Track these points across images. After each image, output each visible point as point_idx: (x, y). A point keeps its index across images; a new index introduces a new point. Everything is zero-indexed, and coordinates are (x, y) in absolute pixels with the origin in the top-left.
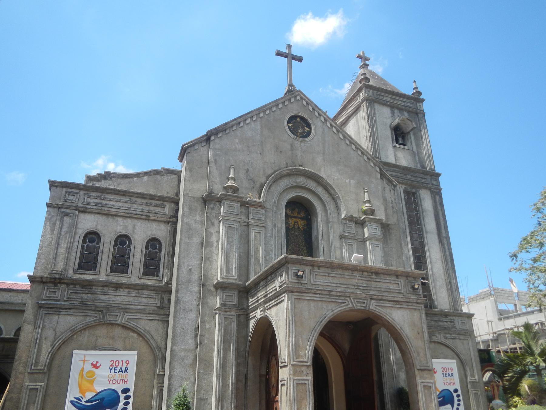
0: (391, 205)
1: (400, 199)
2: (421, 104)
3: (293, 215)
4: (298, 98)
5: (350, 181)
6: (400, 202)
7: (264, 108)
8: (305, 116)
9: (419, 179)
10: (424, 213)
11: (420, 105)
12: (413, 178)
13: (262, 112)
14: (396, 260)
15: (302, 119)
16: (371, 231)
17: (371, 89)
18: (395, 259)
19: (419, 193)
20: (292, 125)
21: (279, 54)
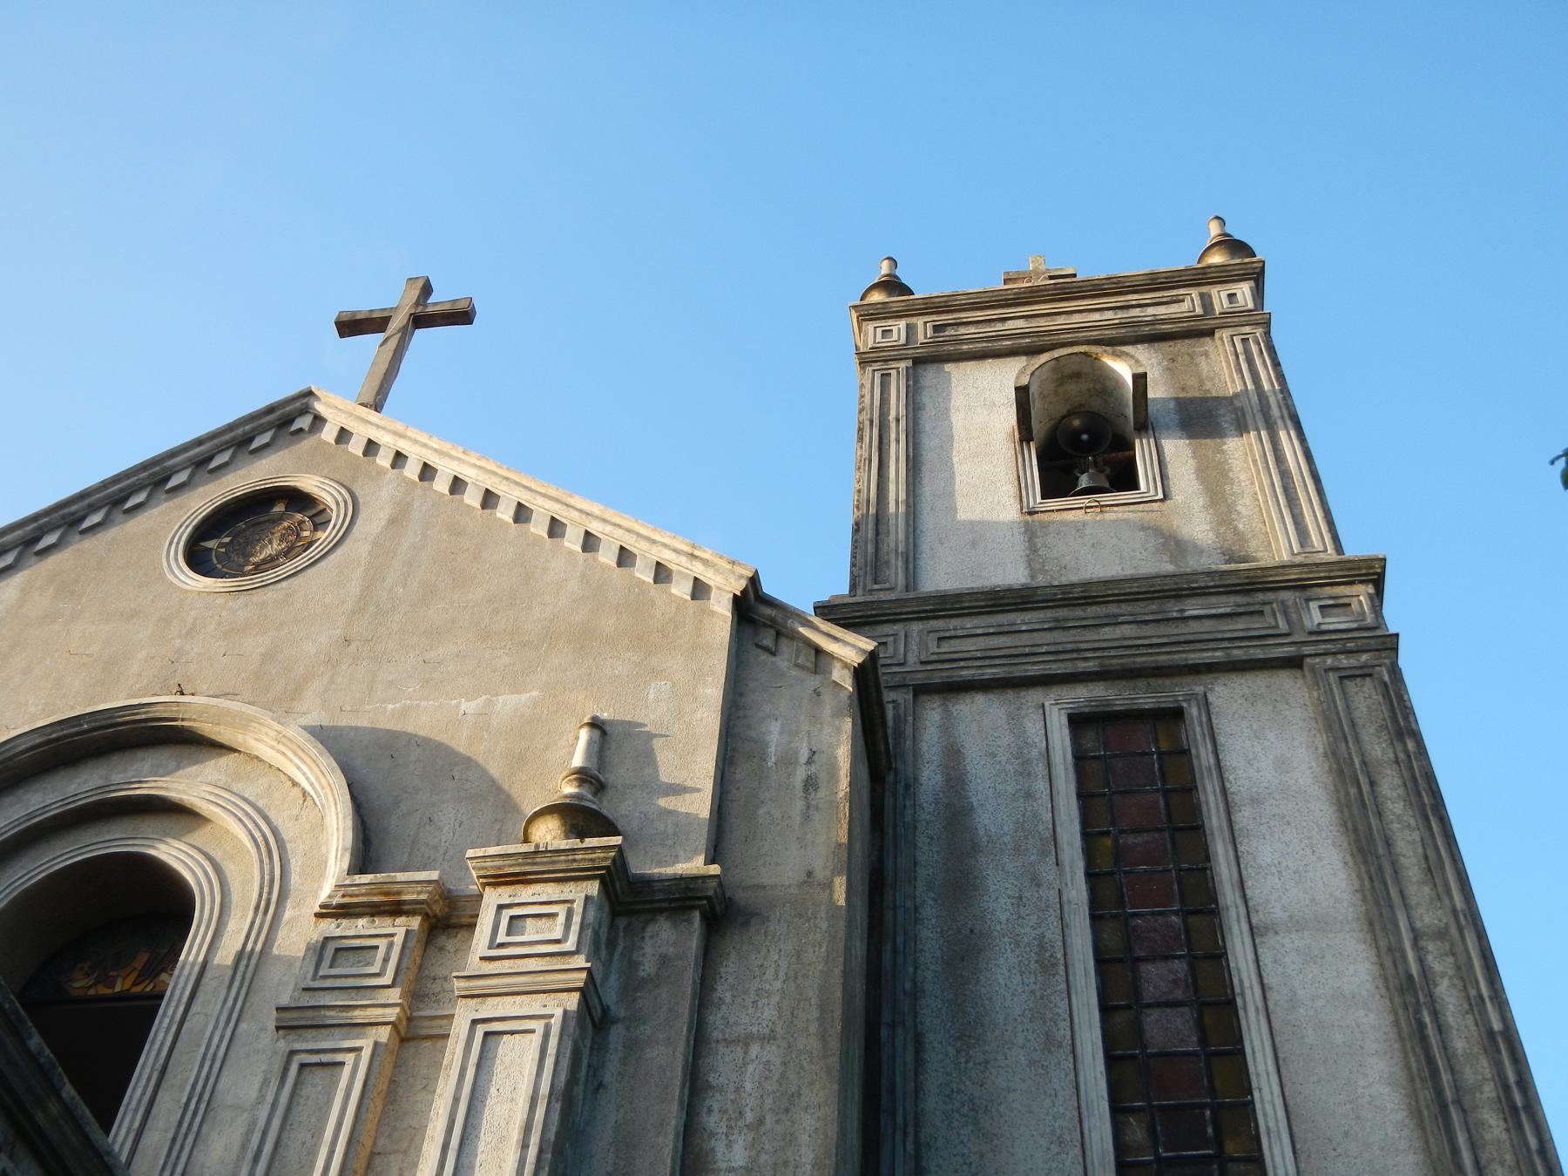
0: (800, 775)
1: (1040, 769)
2: (1244, 290)
3: (103, 991)
4: (304, 422)
5: (490, 703)
6: (1041, 785)
7: (74, 508)
8: (308, 483)
9: (1208, 625)
10: (1243, 817)
11: (1232, 297)
12: (1148, 630)
13: (57, 527)
14: (761, 1122)
15: (298, 500)
16: (502, 937)
17: (898, 315)
18: (749, 1117)
19: (1206, 705)
20: (227, 540)
21: (350, 326)
